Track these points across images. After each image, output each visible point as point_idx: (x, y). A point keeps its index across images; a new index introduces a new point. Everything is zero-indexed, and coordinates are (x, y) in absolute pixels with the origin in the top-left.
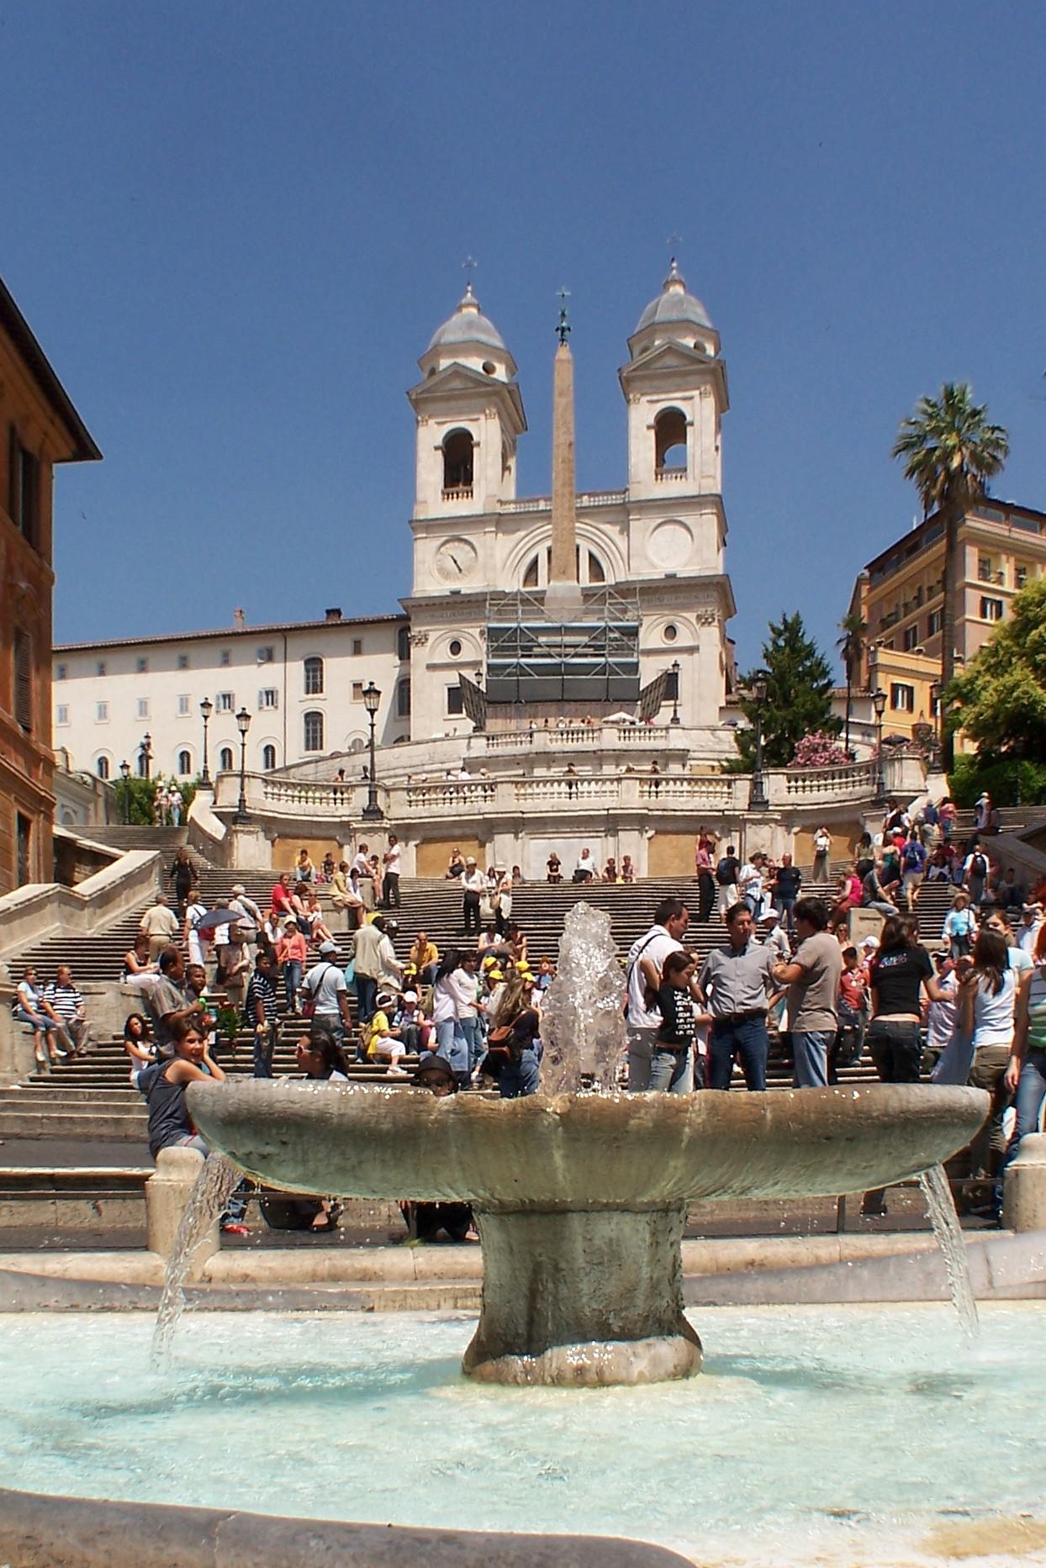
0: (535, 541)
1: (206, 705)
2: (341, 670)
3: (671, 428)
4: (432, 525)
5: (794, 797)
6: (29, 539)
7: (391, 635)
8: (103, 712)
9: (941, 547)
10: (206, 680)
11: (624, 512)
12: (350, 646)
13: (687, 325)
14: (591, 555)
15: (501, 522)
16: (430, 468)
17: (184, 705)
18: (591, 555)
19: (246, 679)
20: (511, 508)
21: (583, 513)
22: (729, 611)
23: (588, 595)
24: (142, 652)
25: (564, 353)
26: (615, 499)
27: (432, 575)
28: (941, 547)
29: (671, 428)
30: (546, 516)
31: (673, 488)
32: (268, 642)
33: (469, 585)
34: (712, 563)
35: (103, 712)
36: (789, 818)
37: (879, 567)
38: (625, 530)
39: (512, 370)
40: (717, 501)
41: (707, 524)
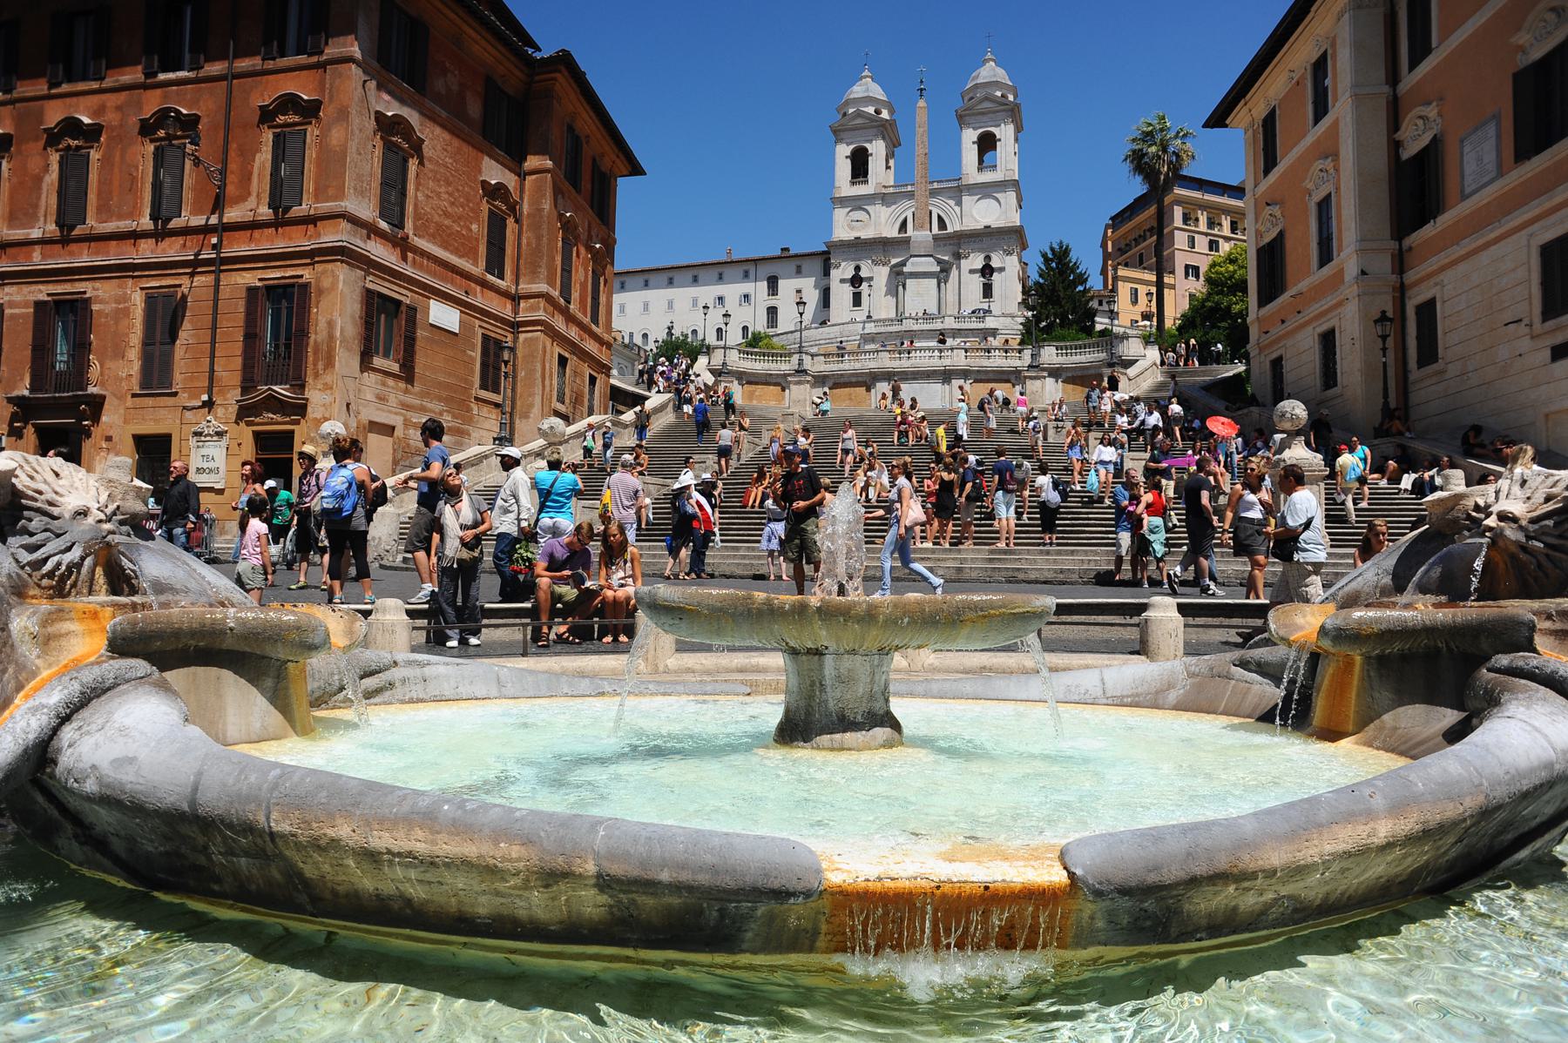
0: (906, 209)
1: (705, 307)
2: (787, 286)
3: (987, 144)
4: (843, 201)
5: (1061, 359)
6: (602, 219)
7: (817, 265)
8: (646, 306)
9: (1153, 209)
10: (707, 293)
11: (959, 191)
12: (794, 269)
13: (997, 85)
14: (939, 217)
15: (885, 199)
16: (844, 168)
17: (695, 302)
18: (939, 217)
19: (732, 291)
20: (891, 190)
21: (934, 193)
22: (1024, 247)
23: (936, 238)
24: (669, 275)
25: (922, 103)
26: (954, 184)
27: (844, 227)
28: (1153, 209)
29: (987, 144)
30: (911, 195)
31: (988, 177)
32: (747, 267)
33: (867, 233)
34: (1015, 219)
35: (646, 306)
36: (1055, 373)
37: (1118, 219)
38: (959, 203)
39: (891, 112)
40: (1015, 184)
41: (1010, 197)
